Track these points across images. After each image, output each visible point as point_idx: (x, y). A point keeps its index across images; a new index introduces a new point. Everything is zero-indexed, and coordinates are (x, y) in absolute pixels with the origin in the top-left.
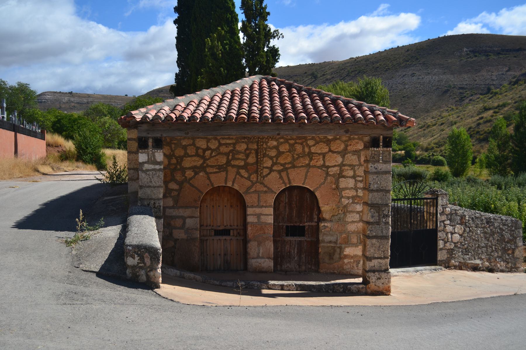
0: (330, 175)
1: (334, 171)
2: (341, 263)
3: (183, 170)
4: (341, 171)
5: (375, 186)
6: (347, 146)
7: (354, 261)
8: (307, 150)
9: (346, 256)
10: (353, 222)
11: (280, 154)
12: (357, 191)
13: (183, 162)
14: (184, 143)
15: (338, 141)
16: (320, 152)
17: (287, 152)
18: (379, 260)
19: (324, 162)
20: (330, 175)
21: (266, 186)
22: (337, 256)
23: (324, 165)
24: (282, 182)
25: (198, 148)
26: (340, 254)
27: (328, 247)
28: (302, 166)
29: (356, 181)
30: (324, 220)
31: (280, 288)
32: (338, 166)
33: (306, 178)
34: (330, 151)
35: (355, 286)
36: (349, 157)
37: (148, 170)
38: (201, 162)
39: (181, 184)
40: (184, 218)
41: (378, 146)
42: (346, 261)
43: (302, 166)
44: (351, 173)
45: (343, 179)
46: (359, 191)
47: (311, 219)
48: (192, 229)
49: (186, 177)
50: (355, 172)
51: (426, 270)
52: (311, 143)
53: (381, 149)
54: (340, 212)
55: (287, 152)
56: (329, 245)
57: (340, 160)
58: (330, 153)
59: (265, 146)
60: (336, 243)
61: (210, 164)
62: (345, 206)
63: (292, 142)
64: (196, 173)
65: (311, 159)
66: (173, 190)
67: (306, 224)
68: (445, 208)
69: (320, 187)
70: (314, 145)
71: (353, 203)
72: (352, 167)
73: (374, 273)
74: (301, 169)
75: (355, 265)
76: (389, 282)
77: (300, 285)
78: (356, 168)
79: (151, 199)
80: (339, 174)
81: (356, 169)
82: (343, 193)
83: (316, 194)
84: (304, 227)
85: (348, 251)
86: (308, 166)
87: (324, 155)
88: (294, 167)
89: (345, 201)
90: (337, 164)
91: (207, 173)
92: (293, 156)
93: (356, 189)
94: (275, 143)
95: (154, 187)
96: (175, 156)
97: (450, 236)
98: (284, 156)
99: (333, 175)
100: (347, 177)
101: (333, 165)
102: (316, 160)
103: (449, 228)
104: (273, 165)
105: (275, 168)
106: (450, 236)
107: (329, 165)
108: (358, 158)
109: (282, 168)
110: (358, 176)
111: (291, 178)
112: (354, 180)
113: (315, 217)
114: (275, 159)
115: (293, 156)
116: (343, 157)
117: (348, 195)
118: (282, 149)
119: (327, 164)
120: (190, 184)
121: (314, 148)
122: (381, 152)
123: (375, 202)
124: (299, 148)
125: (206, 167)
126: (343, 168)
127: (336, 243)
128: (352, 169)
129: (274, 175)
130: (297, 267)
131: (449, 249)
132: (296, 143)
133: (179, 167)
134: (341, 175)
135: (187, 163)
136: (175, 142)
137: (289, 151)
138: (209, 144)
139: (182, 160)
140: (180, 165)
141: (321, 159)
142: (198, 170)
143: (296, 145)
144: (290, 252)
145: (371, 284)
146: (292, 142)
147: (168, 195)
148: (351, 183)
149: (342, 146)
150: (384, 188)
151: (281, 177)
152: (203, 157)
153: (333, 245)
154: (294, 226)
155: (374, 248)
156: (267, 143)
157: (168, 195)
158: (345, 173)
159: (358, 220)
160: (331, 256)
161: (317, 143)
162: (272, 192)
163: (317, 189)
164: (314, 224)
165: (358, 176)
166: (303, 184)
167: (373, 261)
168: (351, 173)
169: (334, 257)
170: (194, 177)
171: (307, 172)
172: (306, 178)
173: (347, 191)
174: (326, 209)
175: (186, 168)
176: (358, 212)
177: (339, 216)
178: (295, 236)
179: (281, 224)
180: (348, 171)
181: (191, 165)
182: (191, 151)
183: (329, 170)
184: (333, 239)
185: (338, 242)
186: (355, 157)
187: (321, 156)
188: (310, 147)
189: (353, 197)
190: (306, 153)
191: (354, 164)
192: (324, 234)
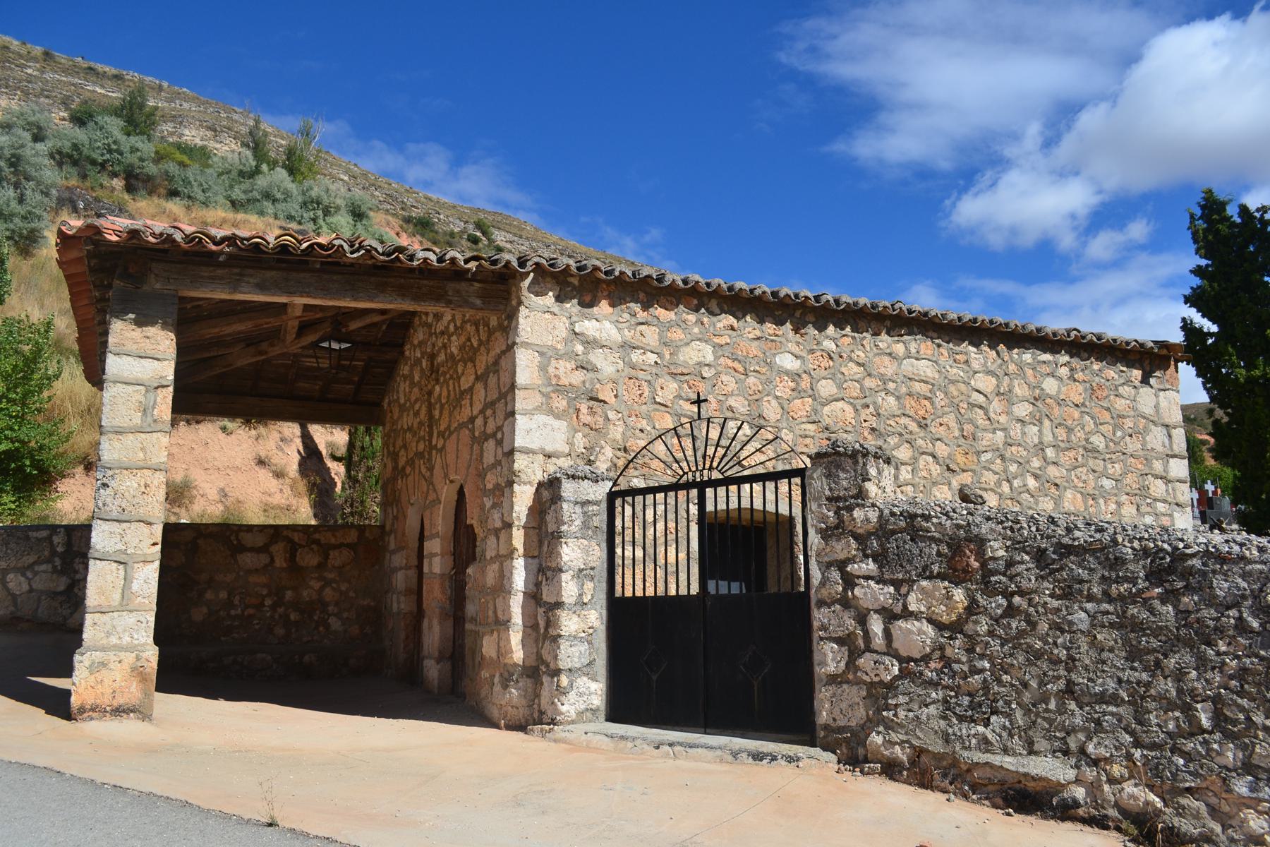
68: (850, 509)
97: (876, 626)
103: (873, 594)
106: (876, 626)
131: (871, 685)
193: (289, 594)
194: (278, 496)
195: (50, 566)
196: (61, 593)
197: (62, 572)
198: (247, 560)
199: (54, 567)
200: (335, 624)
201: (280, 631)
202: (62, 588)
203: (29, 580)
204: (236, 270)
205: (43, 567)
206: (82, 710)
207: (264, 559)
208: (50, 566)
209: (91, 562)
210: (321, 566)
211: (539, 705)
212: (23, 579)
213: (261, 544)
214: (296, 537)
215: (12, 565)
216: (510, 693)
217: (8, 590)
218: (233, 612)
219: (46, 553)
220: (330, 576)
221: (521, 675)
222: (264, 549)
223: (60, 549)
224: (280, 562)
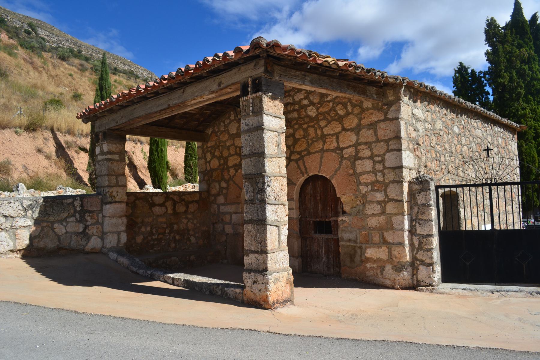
1: (348, 152)
2: (362, 267)
4: (357, 152)
5: (248, 149)
6: (360, 120)
7: (378, 266)
8: (319, 132)
9: (368, 260)
10: (374, 215)
12: (376, 175)
13: (229, 162)
14: (228, 144)
15: (351, 116)
16: (332, 132)
17: (302, 138)
18: (257, 255)
19: (338, 143)
20: (345, 158)
22: (357, 259)
24: (299, 172)
26: (361, 256)
27: (348, 246)
28: (317, 152)
29: (374, 162)
30: (344, 213)
31: (171, 282)
32: (353, 146)
33: (321, 165)
34: (344, 129)
35: (232, 289)
36: (364, 133)
37: (100, 161)
39: (227, 182)
40: (231, 214)
41: (247, 95)
42: (368, 265)
43: (317, 152)
44: (367, 153)
45: (360, 162)
46: (379, 174)
48: (236, 224)
49: (230, 175)
50: (371, 151)
51: (520, 291)
52: (322, 123)
53: (249, 96)
54: (358, 202)
55: (302, 138)
56: (348, 244)
58: (344, 132)
60: (355, 241)
62: (364, 196)
63: (305, 126)
64: (236, 171)
65: (324, 142)
67: (332, 219)
69: (335, 174)
70: (326, 126)
72: (368, 144)
73: (250, 273)
74: (316, 155)
75: (379, 271)
76: (266, 289)
77: (187, 283)
78: (373, 145)
79: (102, 187)
80: (355, 156)
81: (373, 147)
82: (361, 178)
83: (334, 182)
84: (330, 222)
85: (370, 253)
87: (337, 135)
88: (309, 153)
89: (363, 189)
90: (351, 144)
93: (374, 172)
98: (299, 143)
99: (349, 159)
100: (364, 158)
101: (348, 145)
102: (329, 143)
108: (375, 133)
109: (299, 156)
110: (377, 156)
111: (307, 167)
112: (371, 161)
114: (292, 147)
115: (308, 142)
116: (357, 134)
117: (366, 181)
119: (341, 146)
121: (326, 129)
122: (251, 101)
123: (249, 172)
124: (311, 131)
126: (359, 147)
127: (355, 241)
128: (369, 147)
130: (326, 269)
132: (309, 127)
134: (357, 157)
136: (222, 144)
137: (304, 137)
140: (227, 164)
141: (335, 141)
143: (309, 129)
144: (318, 251)
145: (247, 289)
146: (305, 126)
148: (367, 165)
149: (356, 121)
150: (257, 151)
151: (299, 167)
153: (352, 245)
154: (320, 222)
155: (250, 238)
158: (361, 154)
159: (380, 212)
160: (352, 257)
161: (329, 122)
163: (332, 176)
165: (377, 156)
166: (319, 172)
167: (250, 255)
168: (367, 153)
169: (356, 260)
171: (322, 157)
172: (321, 165)
173: (365, 176)
174: (346, 198)
176: (379, 203)
177: (358, 208)
178: (323, 233)
179: (308, 219)
180: (364, 151)
182: (232, 151)
183: (344, 152)
185: (358, 241)
186: (371, 132)
187: (334, 137)
188: (322, 129)
189: (372, 184)
190: (319, 136)
191: (371, 141)
192: (343, 230)
193: (175, 227)
194: (50, 168)
195: (74, 218)
196: (81, 233)
197: (80, 222)
198: (157, 210)
199: (76, 219)
200: (193, 240)
201: (173, 245)
202: (81, 230)
203: (65, 227)
204: (303, 73)
205: (72, 219)
206: (274, 304)
207: (163, 209)
208: (74, 218)
209: (268, 227)
210: (186, 212)
211: (417, 278)
212: (62, 226)
213: (162, 202)
214: (176, 198)
215: (56, 219)
216: (403, 274)
217: (55, 233)
218: (154, 237)
219: (72, 211)
220: (190, 216)
221: (408, 266)
222: (163, 205)
223: (78, 209)
224: (170, 211)
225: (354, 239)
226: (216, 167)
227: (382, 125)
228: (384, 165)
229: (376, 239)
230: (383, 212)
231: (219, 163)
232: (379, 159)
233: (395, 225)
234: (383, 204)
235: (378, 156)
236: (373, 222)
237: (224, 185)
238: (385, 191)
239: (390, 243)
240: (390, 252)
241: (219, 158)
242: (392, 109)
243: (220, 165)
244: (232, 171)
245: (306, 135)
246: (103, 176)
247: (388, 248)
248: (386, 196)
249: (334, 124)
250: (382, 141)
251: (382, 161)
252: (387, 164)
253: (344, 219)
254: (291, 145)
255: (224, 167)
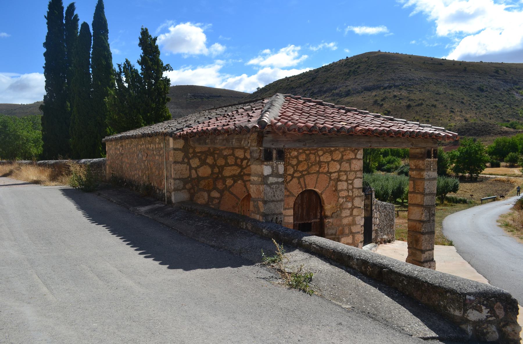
0: (332, 180)
3: (224, 179)
4: (339, 176)
6: (343, 156)
8: (318, 159)
11: (299, 162)
12: (348, 192)
13: (224, 172)
14: (225, 153)
15: (337, 152)
16: (326, 160)
20: (332, 180)
21: (288, 191)
23: (328, 172)
25: (237, 158)
33: (316, 183)
34: (332, 160)
37: (272, 184)
38: (239, 171)
39: (221, 192)
41: (430, 158)
43: (314, 173)
46: (350, 191)
47: (316, 217)
49: (226, 185)
50: (347, 176)
52: (320, 153)
57: (338, 167)
58: (332, 162)
59: (289, 156)
61: (246, 172)
62: (341, 205)
63: (307, 152)
64: (235, 182)
65: (320, 167)
66: (215, 198)
69: (325, 190)
70: (322, 155)
71: (346, 201)
72: (345, 172)
74: (314, 175)
78: (348, 173)
79: (274, 214)
82: (340, 193)
83: (324, 196)
84: (311, 223)
86: (318, 172)
88: (309, 173)
89: (341, 200)
90: (336, 170)
91: (244, 181)
92: (308, 165)
93: (348, 190)
94: (296, 153)
95: (277, 201)
96: (217, 166)
98: (302, 164)
99: (334, 180)
100: (343, 181)
104: (294, 173)
105: (295, 175)
107: (332, 171)
109: (300, 174)
111: (307, 183)
113: (319, 214)
115: (308, 165)
116: (340, 165)
118: (301, 158)
119: (330, 171)
120: (230, 192)
123: (428, 204)
124: (312, 157)
125: (243, 176)
129: (295, 180)
132: (310, 153)
133: (220, 176)
134: (338, 180)
135: (228, 172)
136: (217, 152)
137: (306, 160)
138: (246, 154)
139: (223, 170)
140: (221, 174)
142: (236, 179)
143: (311, 155)
146: (307, 152)
147: (210, 203)
149: (340, 156)
152: (241, 166)
154: (304, 223)
156: (290, 153)
157: (210, 203)
158: (341, 178)
161: (324, 153)
162: (293, 195)
164: (318, 220)
168: (345, 178)
170: (233, 185)
171: (318, 177)
174: (328, 208)
175: (227, 177)
176: (349, 209)
181: (231, 174)
182: (231, 161)
184: (333, 232)
186: (347, 165)
188: (319, 157)
189: (346, 197)
192: (329, 228)
225: (334, 233)
226: (206, 175)
227: (354, 162)
228: (353, 186)
229: (347, 231)
230: (351, 214)
231: (212, 171)
232: (350, 182)
233: (357, 222)
234: (352, 209)
235: (350, 180)
236: (345, 221)
237: (215, 194)
238: (353, 202)
239: (354, 233)
240: (353, 238)
241: (212, 166)
242: (359, 152)
243: (213, 173)
244: (229, 182)
245: (307, 159)
246: (277, 201)
247: (353, 236)
248: (353, 205)
249: (327, 155)
250: (353, 171)
251: (352, 184)
252: (355, 186)
253: (329, 220)
254: (295, 165)
255: (218, 176)
